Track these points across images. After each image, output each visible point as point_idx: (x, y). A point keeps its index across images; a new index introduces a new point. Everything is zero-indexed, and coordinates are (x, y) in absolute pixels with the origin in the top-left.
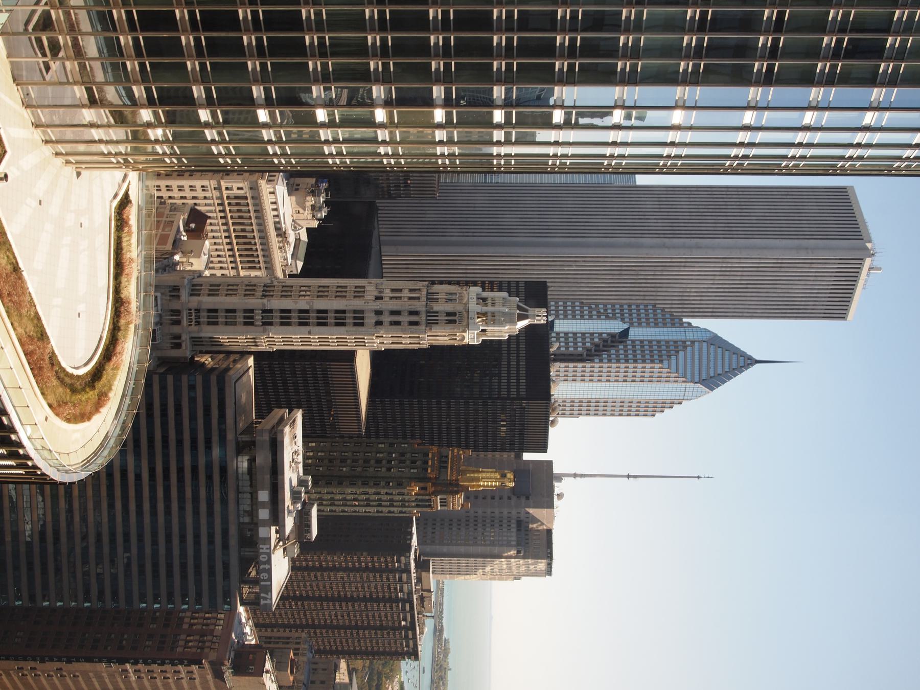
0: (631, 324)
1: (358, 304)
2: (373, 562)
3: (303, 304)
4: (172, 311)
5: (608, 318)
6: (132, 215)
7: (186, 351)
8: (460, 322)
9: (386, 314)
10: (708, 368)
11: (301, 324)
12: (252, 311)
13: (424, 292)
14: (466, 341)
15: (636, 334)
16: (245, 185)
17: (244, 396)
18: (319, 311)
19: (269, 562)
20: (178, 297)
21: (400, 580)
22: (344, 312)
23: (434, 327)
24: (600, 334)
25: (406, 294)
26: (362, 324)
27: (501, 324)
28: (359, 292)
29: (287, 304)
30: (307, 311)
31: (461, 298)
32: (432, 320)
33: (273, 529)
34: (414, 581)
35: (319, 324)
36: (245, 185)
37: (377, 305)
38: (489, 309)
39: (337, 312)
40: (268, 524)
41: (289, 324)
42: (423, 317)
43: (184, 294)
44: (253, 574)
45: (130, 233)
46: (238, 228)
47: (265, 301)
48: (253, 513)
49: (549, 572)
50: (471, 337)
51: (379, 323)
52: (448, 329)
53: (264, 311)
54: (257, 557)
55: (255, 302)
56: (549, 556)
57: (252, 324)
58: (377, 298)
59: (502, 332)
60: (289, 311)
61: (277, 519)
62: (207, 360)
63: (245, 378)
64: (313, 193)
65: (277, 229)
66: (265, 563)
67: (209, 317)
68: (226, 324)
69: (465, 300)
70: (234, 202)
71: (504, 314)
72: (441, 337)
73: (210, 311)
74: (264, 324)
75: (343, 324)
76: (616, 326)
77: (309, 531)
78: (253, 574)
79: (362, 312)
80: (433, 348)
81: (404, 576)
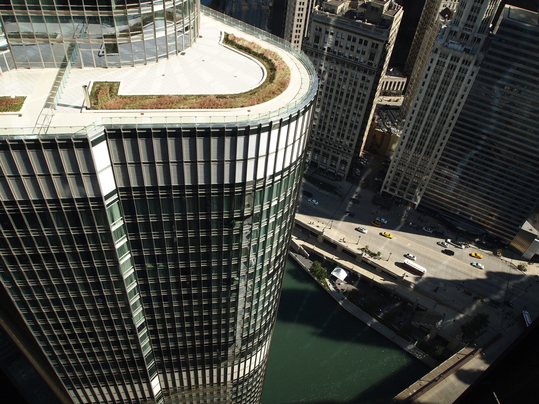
4: (461, 37)
7: (483, 37)
17: (522, 15)
20: (456, 32)
43: (456, 29)
63: (511, 11)
68: (478, 13)
73: (468, 19)
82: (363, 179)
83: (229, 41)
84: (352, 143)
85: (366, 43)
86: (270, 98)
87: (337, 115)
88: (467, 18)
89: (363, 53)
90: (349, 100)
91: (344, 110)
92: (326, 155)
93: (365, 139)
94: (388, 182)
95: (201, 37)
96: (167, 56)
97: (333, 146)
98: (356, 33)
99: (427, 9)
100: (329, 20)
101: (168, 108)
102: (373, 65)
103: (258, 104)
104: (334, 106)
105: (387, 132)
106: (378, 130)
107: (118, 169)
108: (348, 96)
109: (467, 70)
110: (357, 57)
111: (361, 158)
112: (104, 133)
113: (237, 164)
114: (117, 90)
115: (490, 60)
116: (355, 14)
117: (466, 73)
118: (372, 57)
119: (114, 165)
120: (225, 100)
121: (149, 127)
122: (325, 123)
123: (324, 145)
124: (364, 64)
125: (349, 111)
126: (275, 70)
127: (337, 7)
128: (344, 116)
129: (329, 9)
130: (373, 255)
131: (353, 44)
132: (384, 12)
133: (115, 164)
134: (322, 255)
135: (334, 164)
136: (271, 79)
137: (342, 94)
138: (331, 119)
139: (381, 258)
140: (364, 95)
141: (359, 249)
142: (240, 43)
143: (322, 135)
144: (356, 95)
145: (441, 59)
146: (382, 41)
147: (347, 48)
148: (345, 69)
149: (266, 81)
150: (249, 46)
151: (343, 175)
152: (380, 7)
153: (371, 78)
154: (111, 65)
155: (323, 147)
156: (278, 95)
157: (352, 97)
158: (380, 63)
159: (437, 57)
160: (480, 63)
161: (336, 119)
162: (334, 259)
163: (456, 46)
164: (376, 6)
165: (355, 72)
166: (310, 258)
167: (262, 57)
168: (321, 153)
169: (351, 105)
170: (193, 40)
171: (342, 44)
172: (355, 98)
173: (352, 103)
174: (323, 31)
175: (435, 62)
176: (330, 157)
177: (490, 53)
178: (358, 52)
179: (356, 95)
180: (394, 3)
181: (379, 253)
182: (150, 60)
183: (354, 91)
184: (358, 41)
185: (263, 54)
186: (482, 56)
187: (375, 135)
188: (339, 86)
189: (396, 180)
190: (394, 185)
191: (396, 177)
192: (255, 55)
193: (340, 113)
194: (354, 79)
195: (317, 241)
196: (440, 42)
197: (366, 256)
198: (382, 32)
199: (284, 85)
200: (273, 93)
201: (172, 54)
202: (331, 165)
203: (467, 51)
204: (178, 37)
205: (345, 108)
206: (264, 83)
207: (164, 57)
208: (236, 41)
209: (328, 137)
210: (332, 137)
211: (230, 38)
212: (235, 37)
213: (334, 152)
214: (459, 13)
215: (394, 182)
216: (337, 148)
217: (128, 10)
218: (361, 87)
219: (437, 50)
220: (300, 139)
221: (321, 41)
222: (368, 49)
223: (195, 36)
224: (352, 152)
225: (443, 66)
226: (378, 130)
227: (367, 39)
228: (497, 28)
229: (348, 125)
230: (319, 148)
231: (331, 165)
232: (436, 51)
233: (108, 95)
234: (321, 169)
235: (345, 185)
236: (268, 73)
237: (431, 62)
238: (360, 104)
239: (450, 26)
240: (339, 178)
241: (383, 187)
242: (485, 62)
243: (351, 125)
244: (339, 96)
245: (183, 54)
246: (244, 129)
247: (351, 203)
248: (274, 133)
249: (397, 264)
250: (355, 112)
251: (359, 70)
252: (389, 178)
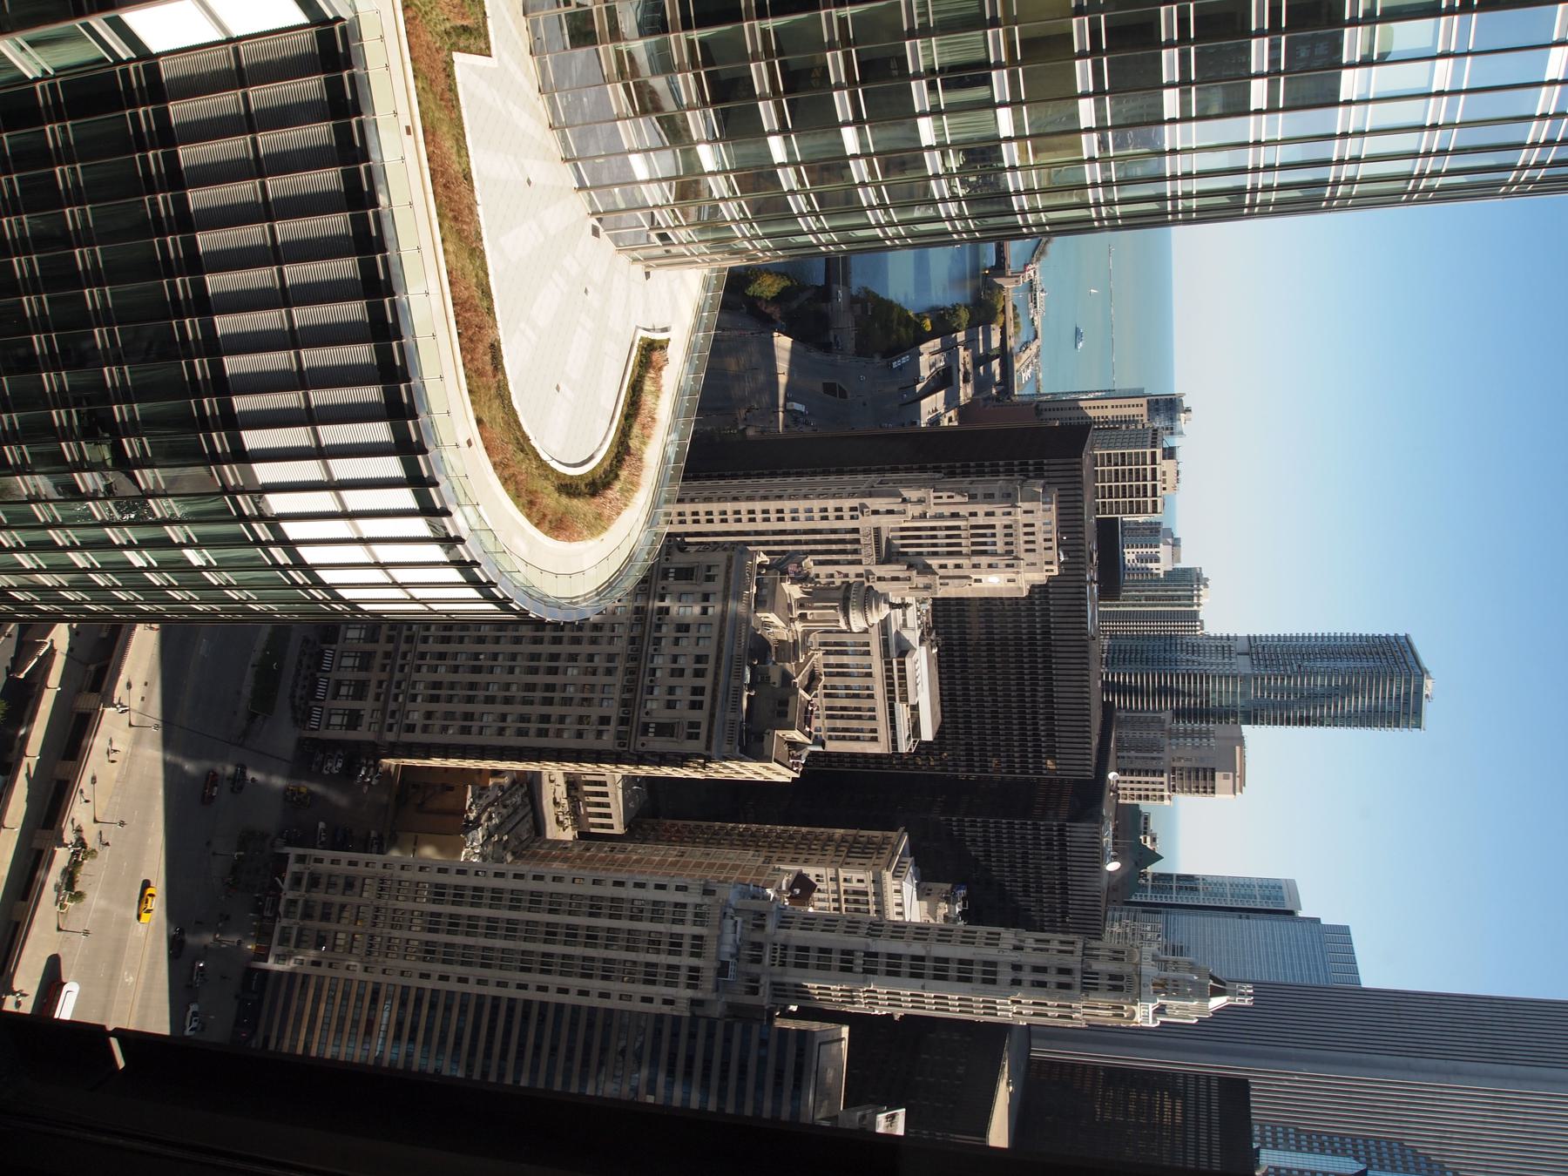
0: (1370, 1166)
1: (990, 953)
5: (1334, 1153)
7: (764, 998)
8: (1129, 989)
9: (1027, 969)
11: (913, 975)
16: (868, 876)
17: (830, 1074)
18: (937, 959)
20: (762, 927)
22: (971, 962)
23: (1092, 993)
25: (1055, 945)
26: (994, 982)
28: (993, 940)
29: (898, 947)
30: (922, 959)
31: (1131, 956)
35: (936, 977)
36: (868, 876)
37: (1015, 957)
39: (961, 962)
41: (897, 974)
42: (1077, 979)
43: (771, 924)
47: (869, 940)
50: (1144, 1014)
51: (1016, 982)
52: (1111, 1000)
53: (868, 954)
55: (856, 942)
57: (850, 970)
58: (1016, 948)
63: (835, 1046)
64: (947, 900)
67: (797, 957)
68: (818, 967)
69: (1137, 960)
70: (852, 897)
71: (1192, 983)
73: (799, 949)
74: (866, 971)
75: (968, 980)
79: (994, 964)
82: (315, 787)
83: (649, 354)
84: (418, 730)
85: (695, 705)
86: (516, 497)
87: (491, 670)
88: (801, 944)
89: (670, 705)
90: (539, 694)
91: (507, 686)
92: (366, 661)
93: (436, 762)
94: (320, 861)
95: (648, 275)
96: (582, 187)
97: (398, 676)
98: (716, 675)
99: (804, 837)
100: (738, 597)
101: (439, 207)
102: (643, 739)
103: (495, 465)
104: (513, 657)
105: (468, 821)
106: (470, 794)
107: (220, 60)
108: (550, 687)
109: (675, 985)
110: (656, 692)
111: (377, 765)
112: (331, 16)
113: (302, 429)
114: (467, 50)
115: (710, 1035)
116: (763, 661)
117: (667, 984)
118: (664, 730)
119: (230, 46)
120: (489, 368)
121: (374, 156)
122: (461, 640)
123: (397, 649)
124: (643, 714)
125: (508, 701)
126: (593, 495)
127: (772, 610)
128: (493, 690)
129: (765, 592)
130: (70, 876)
131: (689, 672)
132: (780, 733)
133: (236, 52)
134: (32, 720)
135: (344, 691)
136: (568, 488)
137: (553, 671)
138: (476, 656)
139: (62, 907)
140: (559, 733)
141: (79, 830)
142: (648, 386)
143: (425, 640)
144: (555, 711)
145: (690, 910)
146: (708, 748)
147: (675, 659)
148: (620, 664)
149: (559, 476)
150: (644, 412)
151: (314, 724)
152: (790, 719)
153: (608, 741)
154: (533, 28)
155: (390, 647)
156: (528, 516)
157: (548, 702)
158: (653, 754)
159: (692, 898)
160: (699, 1012)
161: (477, 670)
162: (26, 760)
163: (729, 938)
164: (790, 709)
165: (617, 694)
166: (11, 682)
167: (622, 451)
168: (369, 647)
169: (527, 702)
170: (635, 254)
171: (683, 642)
172: (546, 710)
173: (532, 703)
174: (708, 587)
175: (680, 897)
176: (362, 675)
177: (729, 1028)
178: (671, 690)
179: (555, 711)
180: (805, 754)
181: (79, 896)
182: (564, 139)
183: (567, 701)
184: (699, 682)
185: (629, 454)
186: (716, 1011)
187: (451, 789)
188: (573, 657)
189: (331, 885)
190: (315, 881)
191: (341, 882)
192: (624, 434)
193: (499, 676)
194: (596, 696)
195: (79, 691)
196: (730, 894)
197: (62, 857)
198: (730, 742)
199: (557, 526)
200: (532, 503)
201: (591, 202)
202: (339, 684)
203: (723, 969)
204: (639, 214)
205: (514, 688)
206: (553, 470)
207: (580, 179)
208: (652, 374)
209: (423, 656)
210: (424, 669)
211: (656, 356)
212: (660, 369)
213: (380, 683)
214: (809, 922)
215: (324, 880)
216: (394, 691)
217: (690, 76)
218: (581, 720)
219: (712, 893)
220: (413, 600)
221: (683, 586)
222: (683, 713)
223: (646, 259)
224: (390, 737)
225: (674, 922)
226: (470, 794)
227: (707, 706)
228: (791, 1025)
229: (469, 708)
230: (382, 638)
231: (339, 684)
232: (707, 892)
233: (448, 25)
234: (322, 654)
235: (285, 737)
236: (581, 477)
237: (678, 888)
238: (533, 726)
239: (774, 908)
240: (302, 716)
241: (301, 851)
242: (703, 1023)
243: (468, 716)
244: (544, 664)
245: (595, 232)
246: (414, 438)
247: (230, 769)
248: (419, 527)
249: (54, 963)
250: (509, 719)
251: (625, 703)
252: (333, 862)
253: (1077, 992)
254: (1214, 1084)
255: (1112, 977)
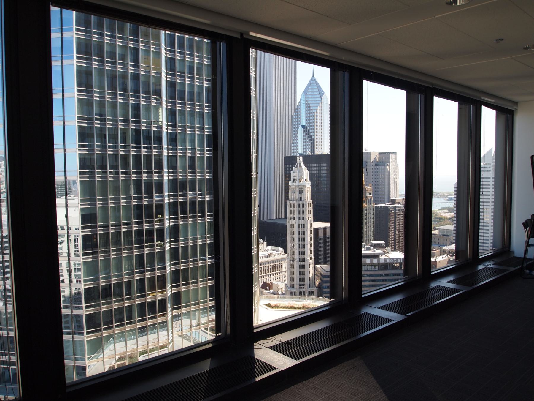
1: (296, 226)
2: (392, 221)
3: (297, 247)
5: (297, 133)
6: (273, 303)
7: (315, 290)
9: (300, 216)
10: (316, 95)
12: (300, 265)
13: (292, 202)
14: (309, 186)
15: (303, 122)
18: (299, 241)
19: (393, 259)
21: (399, 210)
24: (304, 136)
25: (292, 209)
26: (304, 225)
27: (303, 174)
28: (292, 226)
30: (299, 245)
31: (294, 188)
32: (302, 199)
33: (380, 257)
34: (399, 205)
35: (304, 241)
37: (297, 219)
38: (297, 178)
39: (299, 234)
40: (379, 260)
41: (304, 252)
42: (301, 203)
43: (294, 290)
44: (398, 265)
45: (280, 304)
46: (267, 271)
47: (296, 261)
48: (374, 265)
49: (395, 153)
50: (308, 184)
51: (303, 219)
53: (300, 261)
54: (391, 263)
55: (296, 264)
56: (389, 153)
57: (304, 266)
58: (294, 219)
59: (306, 173)
60: (299, 252)
61: (376, 256)
62: (317, 282)
63: (324, 268)
65: (267, 257)
66: (394, 260)
68: (304, 275)
71: (299, 172)
72: (308, 195)
73: (300, 281)
74: (304, 261)
75: (304, 232)
76: (301, 130)
77: (381, 244)
78: (398, 265)
79: (299, 225)
80: (312, 199)
81: (397, 209)
253: (304, 202)
254: (287, 166)
255: (300, 193)
